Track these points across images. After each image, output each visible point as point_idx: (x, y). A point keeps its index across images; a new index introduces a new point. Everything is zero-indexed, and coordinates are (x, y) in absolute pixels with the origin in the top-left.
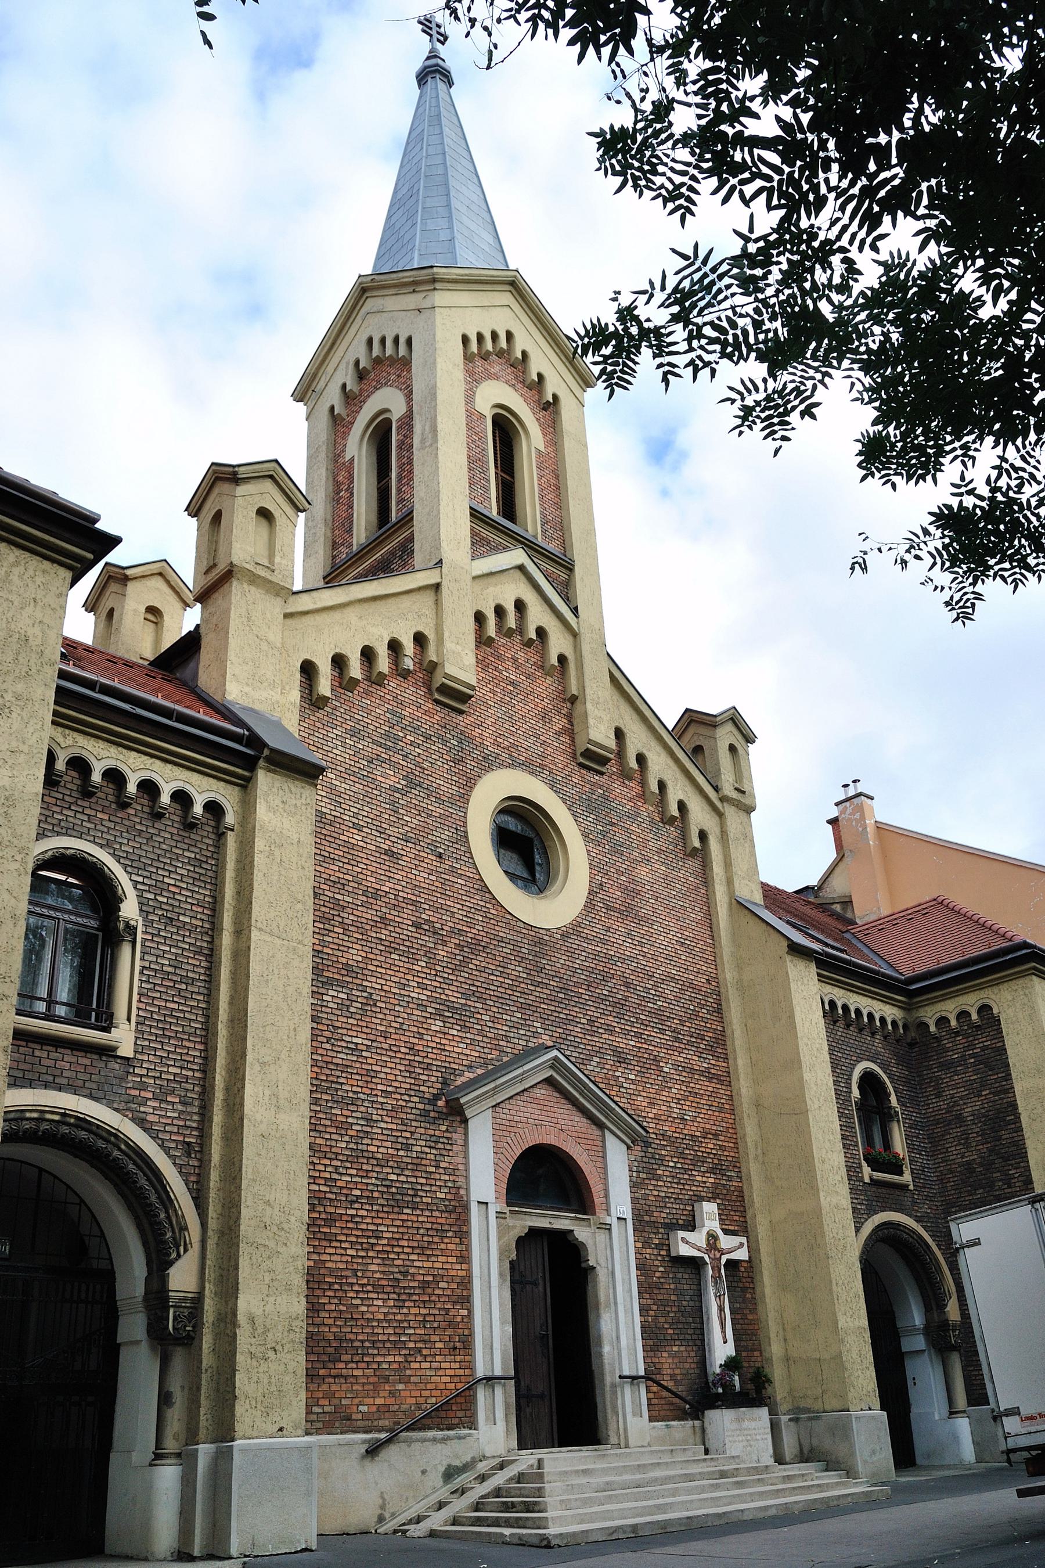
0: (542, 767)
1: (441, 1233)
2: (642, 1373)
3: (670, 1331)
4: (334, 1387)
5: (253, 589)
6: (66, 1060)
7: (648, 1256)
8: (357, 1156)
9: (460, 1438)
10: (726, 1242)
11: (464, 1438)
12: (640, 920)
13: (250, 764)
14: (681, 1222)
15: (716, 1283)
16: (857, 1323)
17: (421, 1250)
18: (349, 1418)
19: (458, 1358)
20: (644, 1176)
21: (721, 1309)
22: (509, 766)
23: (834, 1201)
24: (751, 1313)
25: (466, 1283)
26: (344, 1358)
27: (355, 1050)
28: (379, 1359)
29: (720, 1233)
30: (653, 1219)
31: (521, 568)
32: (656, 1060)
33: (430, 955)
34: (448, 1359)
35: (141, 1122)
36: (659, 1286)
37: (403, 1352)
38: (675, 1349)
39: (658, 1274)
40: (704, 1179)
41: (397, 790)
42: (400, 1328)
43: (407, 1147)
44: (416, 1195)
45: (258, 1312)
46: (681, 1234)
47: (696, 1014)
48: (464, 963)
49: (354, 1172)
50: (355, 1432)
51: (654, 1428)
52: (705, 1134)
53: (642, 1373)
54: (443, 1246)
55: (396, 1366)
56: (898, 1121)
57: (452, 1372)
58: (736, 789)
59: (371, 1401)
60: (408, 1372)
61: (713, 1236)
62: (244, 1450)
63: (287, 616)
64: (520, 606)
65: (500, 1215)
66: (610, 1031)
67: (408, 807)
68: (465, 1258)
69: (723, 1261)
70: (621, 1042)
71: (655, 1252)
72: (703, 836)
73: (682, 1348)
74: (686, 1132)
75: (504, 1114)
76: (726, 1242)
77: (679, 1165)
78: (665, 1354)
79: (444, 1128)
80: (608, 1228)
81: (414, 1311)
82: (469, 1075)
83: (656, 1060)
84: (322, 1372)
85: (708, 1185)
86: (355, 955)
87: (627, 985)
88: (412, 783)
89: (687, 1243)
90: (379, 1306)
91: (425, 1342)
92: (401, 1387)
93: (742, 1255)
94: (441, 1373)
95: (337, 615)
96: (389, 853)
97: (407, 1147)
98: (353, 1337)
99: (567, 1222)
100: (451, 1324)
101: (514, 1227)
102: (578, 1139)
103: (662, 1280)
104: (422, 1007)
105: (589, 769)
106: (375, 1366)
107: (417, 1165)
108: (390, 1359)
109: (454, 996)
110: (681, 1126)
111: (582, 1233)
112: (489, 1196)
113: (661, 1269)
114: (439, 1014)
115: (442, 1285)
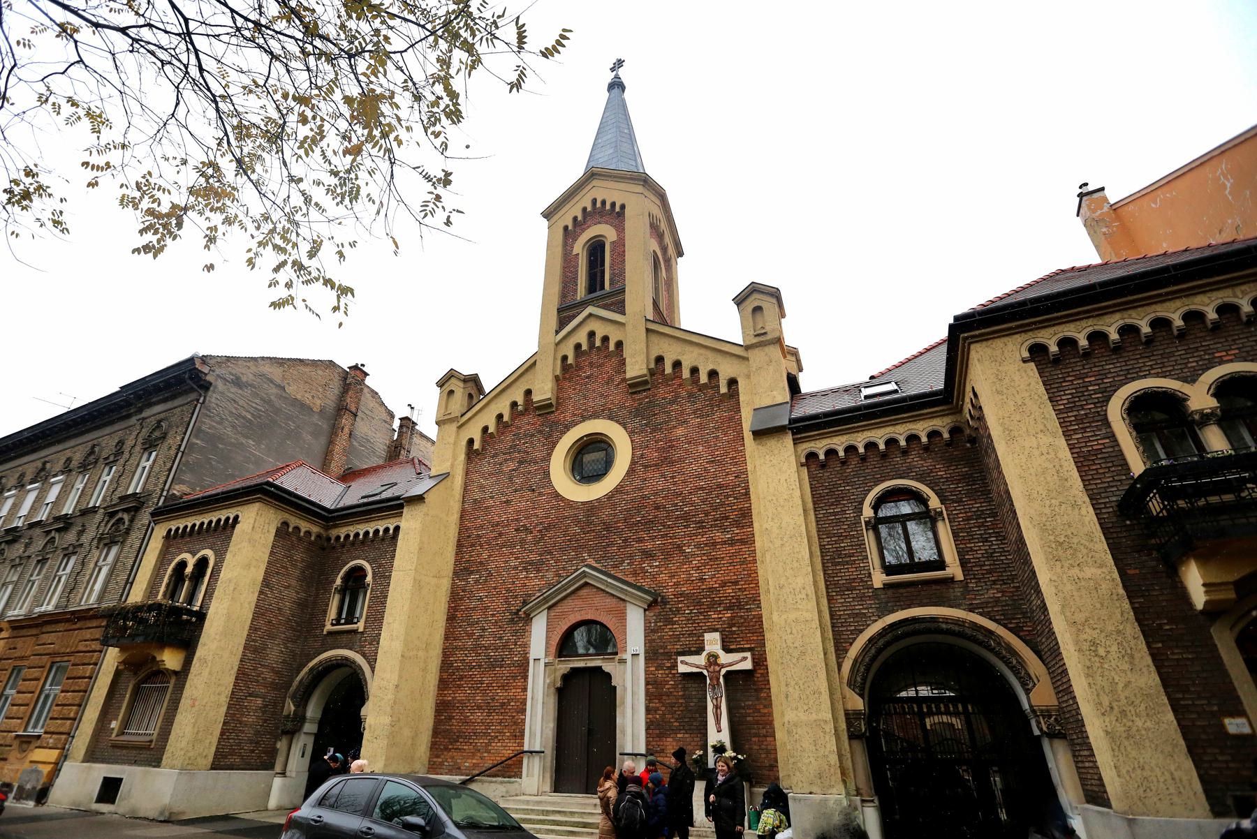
0: (603, 410)
1: (515, 678)
2: (643, 750)
3: (676, 724)
4: (455, 754)
5: (446, 426)
7: (660, 675)
8: (475, 648)
9: (510, 783)
10: (724, 658)
11: (513, 782)
12: (672, 463)
13: (401, 506)
14: (692, 649)
15: (714, 688)
16: (814, 717)
17: (503, 687)
18: (459, 768)
19: (517, 741)
20: (661, 624)
21: (717, 707)
22: (581, 422)
23: (792, 616)
24: (765, 707)
25: (524, 702)
27: (481, 599)
28: (477, 741)
29: (721, 653)
30: (666, 651)
32: (679, 547)
33: (523, 542)
34: (512, 741)
36: (668, 695)
39: (667, 687)
40: (720, 616)
42: (488, 726)
43: (500, 638)
45: (373, 723)
46: (680, 658)
47: (722, 504)
48: (542, 538)
50: (462, 775)
52: (724, 584)
53: (643, 751)
55: (484, 744)
56: (944, 519)
57: (513, 748)
58: (756, 336)
59: (470, 761)
60: (490, 748)
61: (713, 656)
63: (459, 427)
64: (592, 335)
65: (546, 665)
66: (640, 540)
67: (518, 477)
68: (525, 689)
69: (723, 671)
70: (649, 545)
71: (667, 672)
72: (733, 382)
73: (687, 736)
74: (704, 587)
75: (558, 609)
76: (724, 658)
80: (623, 661)
81: (496, 717)
82: (538, 594)
83: (679, 547)
84: (450, 747)
85: (724, 619)
87: (657, 508)
88: (521, 463)
89: (686, 664)
90: (478, 716)
91: (500, 733)
92: (486, 755)
93: (747, 665)
94: (507, 748)
95: (486, 410)
96: (507, 502)
97: (500, 638)
98: (464, 730)
99: (600, 661)
100: (516, 723)
101: (561, 669)
102: (609, 611)
103: (671, 690)
104: (516, 568)
105: (639, 392)
107: (505, 646)
108: (481, 741)
110: (699, 584)
111: (607, 667)
112: (542, 654)
114: (525, 569)
115: (512, 704)
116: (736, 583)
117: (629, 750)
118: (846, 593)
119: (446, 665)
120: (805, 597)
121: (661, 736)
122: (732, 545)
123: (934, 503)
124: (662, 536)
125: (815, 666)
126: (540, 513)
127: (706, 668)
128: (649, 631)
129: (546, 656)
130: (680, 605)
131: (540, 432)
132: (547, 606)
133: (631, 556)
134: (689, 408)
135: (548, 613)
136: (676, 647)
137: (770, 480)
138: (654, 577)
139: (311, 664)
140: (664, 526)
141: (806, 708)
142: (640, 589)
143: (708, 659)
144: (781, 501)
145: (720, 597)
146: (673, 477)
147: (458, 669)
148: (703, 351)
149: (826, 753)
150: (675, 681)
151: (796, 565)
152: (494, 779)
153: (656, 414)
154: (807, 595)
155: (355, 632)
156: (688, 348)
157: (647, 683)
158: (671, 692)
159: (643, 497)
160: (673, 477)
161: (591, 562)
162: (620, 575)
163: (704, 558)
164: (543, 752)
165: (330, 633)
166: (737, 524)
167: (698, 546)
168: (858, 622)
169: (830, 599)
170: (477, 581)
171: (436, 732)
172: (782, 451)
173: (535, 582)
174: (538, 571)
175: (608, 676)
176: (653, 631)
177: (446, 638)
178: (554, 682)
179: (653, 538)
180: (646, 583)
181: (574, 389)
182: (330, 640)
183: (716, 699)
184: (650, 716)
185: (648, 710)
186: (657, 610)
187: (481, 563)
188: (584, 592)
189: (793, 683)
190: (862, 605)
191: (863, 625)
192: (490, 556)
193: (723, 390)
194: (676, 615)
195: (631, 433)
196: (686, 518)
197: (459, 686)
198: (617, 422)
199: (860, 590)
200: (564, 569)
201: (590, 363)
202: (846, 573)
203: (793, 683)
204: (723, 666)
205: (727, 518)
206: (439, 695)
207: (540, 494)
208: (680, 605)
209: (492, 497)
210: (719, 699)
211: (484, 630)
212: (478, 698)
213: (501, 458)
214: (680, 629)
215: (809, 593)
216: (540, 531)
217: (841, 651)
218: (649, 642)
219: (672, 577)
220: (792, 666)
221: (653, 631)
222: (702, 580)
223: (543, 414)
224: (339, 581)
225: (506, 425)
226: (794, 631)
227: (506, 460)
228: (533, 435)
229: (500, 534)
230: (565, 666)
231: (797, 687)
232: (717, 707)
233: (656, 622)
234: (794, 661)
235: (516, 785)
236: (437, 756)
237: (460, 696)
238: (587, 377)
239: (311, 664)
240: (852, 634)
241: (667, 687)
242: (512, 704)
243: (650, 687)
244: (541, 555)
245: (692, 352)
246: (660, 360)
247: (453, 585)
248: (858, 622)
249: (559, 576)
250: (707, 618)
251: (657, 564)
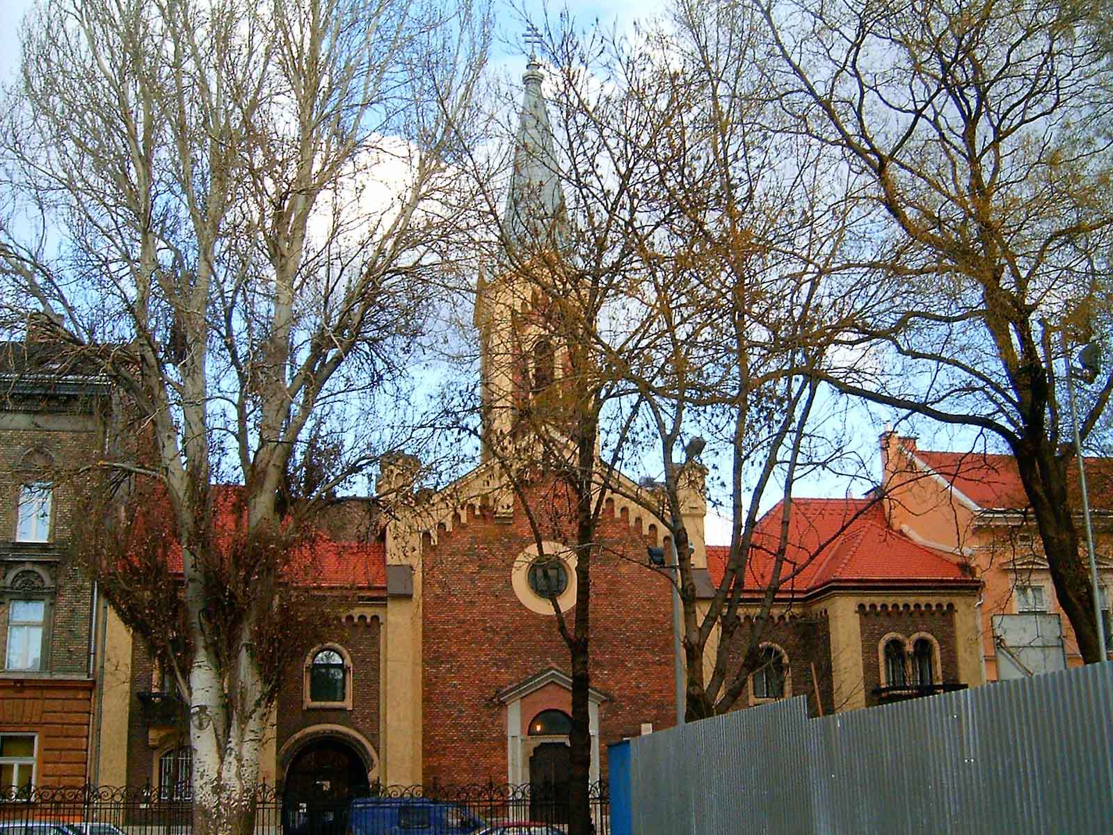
1: (495, 749)
6: (333, 714)
12: (618, 595)
25: (505, 767)
33: (491, 642)
35: (357, 730)
47: (653, 634)
48: (508, 641)
52: (653, 692)
67: (480, 579)
68: (505, 758)
82: (509, 687)
86: (454, 649)
87: (606, 630)
88: (481, 567)
97: (479, 719)
109: (502, 655)
116: (661, 691)
122: (660, 665)
123: (786, 660)
126: (506, 618)
129: (522, 733)
138: (604, 683)
139: (297, 736)
147: (440, 742)
157: (600, 754)
161: (553, 665)
165: (309, 710)
166: (662, 650)
170: (449, 670)
173: (506, 676)
174: (508, 668)
176: (604, 720)
177: (425, 716)
178: (529, 752)
186: (607, 705)
187: (451, 655)
192: (459, 650)
196: (628, 641)
197: (444, 755)
200: (531, 668)
205: (656, 645)
211: (461, 711)
216: (507, 634)
219: (617, 683)
221: (604, 720)
222: (638, 687)
225: (464, 527)
229: (468, 632)
230: (536, 742)
237: (445, 762)
239: (297, 736)
244: (509, 654)
247: (424, 671)
249: (528, 674)
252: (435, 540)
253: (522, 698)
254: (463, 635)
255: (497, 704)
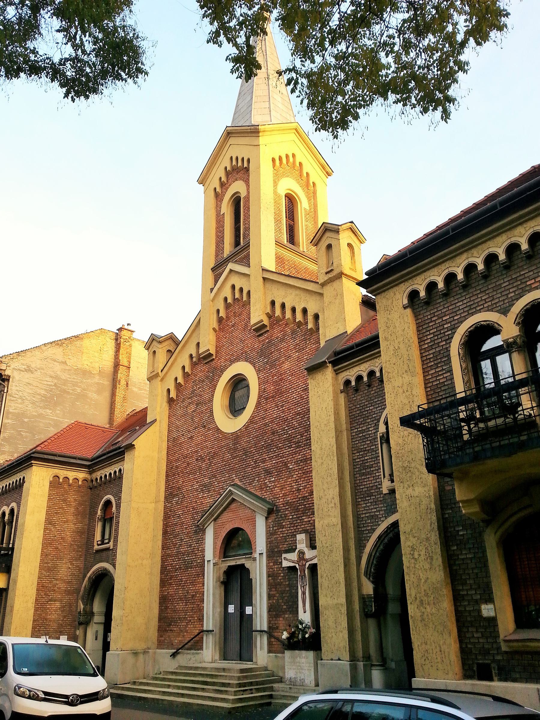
2: (265, 628)
3: (285, 607)
4: (170, 634)
7: (275, 569)
15: (302, 579)
16: (335, 601)
20: (276, 528)
21: (304, 593)
22: (230, 365)
23: (326, 522)
26: (173, 624)
29: (306, 550)
31: (231, 271)
36: (280, 584)
37: (186, 621)
38: (286, 616)
39: (280, 578)
40: (309, 519)
41: (194, 411)
42: (186, 612)
44: (192, 563)
46: (284, 555)
49: (177, 560)
51: (270, 656)
54: (198, 581)
59: (177, 638)
62: (111, 654)
64: (233, 287)
66: (264, 461)
70: (268, 464)
72: (316, 317)
73: (291, 616)
74: (300, 496)
75: (219, 521)
77: (295, 516)
78: (281, 619)
79: (201, 535)
83: (286, 464)
89: (287, 560)
91: (192, 617)
96: (191, 438)
99: (244, 560)
106: (179, 627)
109: (206, 480)
113: (282, 575)
117: (259, 629)
118: (367, 499)
119: (164, 570)
120: (333, 506)
121: (277, 616)
124: (277, 456)
125: (337, 561)
127: (298, 562)
128: (270, 534)
130: (286, 512)
131: (207, 377)
132: (213, 519)
133: (258, 475)
134: (292, 344)
135: (214, 524)
136: (284, 546)
137: (316, 410)
139: (88, 575)
140: (277, 448)
141: (331, 595)
142: (264, 500)
143: (299, 555)
144: (323, 426)
145: (309, 504)
146: (282, 406)
148: (298, 292)
149: (342, 630)
150: (284, 574)
151: (329, 479)
152: (189, 651)
153: (271, 353)
154: (335, 504)
155: (108, 549)
156: (290, 291)
157: (269, 576)
158: (282, 582)
159: (266, 425)
160: (282, 406)
162: (252, 491)
163: (300, 472)
164: (213, 631)
165: (98, 551)
167: (296, 463)
168: (373, 523)
169: (356, 504)
171: (160, 620)
172: (325, 383)
175: (248, 571)
178: (219, 577)
179: (271, 458)
180: (267, 496)
181: (226, 338)
182: (98, 556)
183: (303, 587)
184: (271, 601)
185: (270, 597)
186: (273, 517)
188: (233, 505)
189: (325, 575)
190: (376, 508)
191: (376, 525)
193: (310, 325)
194: (284, 520)
195: (258, 371)
198: (250, 362)
199: (375, 496)
201: (234, 313)
202: (369, 482)
203: (325, 575)
204: (307, 561)
206: (161, 591)
207: (209, 429)
208: (286, 512)
209: (183, 435)
210: (305, 587)
212: (180, 592)
213: (186, 403)
214: (287, 532)
215: (336, 501)
217: (360, 546)
218: (269, 543)
219: (281, 490)
220: (324, 562)
222: (298, 490)
223: (208, 362)
224: (99, 512)
226: (327, 534)
227: (190, 403)
228: (203, 381)
231: (327, 578)
232: (304, 593)
233: (273, 527)
234: (326, 558)
235: (200, 655)
236: (161, 636)
238: (233, 326)
239: (88, 575)
240: (369, 533)
241: (280, 578)
242: (198, 595)
243: (270, 578)
245: (291, 293)
246: (273, 303)
248: (373, 523)
250: (302, 521)
251: (274, 479)
252: (173, 394)
253: (215, 520)
254: (186, 468)
255: (201, 530)
